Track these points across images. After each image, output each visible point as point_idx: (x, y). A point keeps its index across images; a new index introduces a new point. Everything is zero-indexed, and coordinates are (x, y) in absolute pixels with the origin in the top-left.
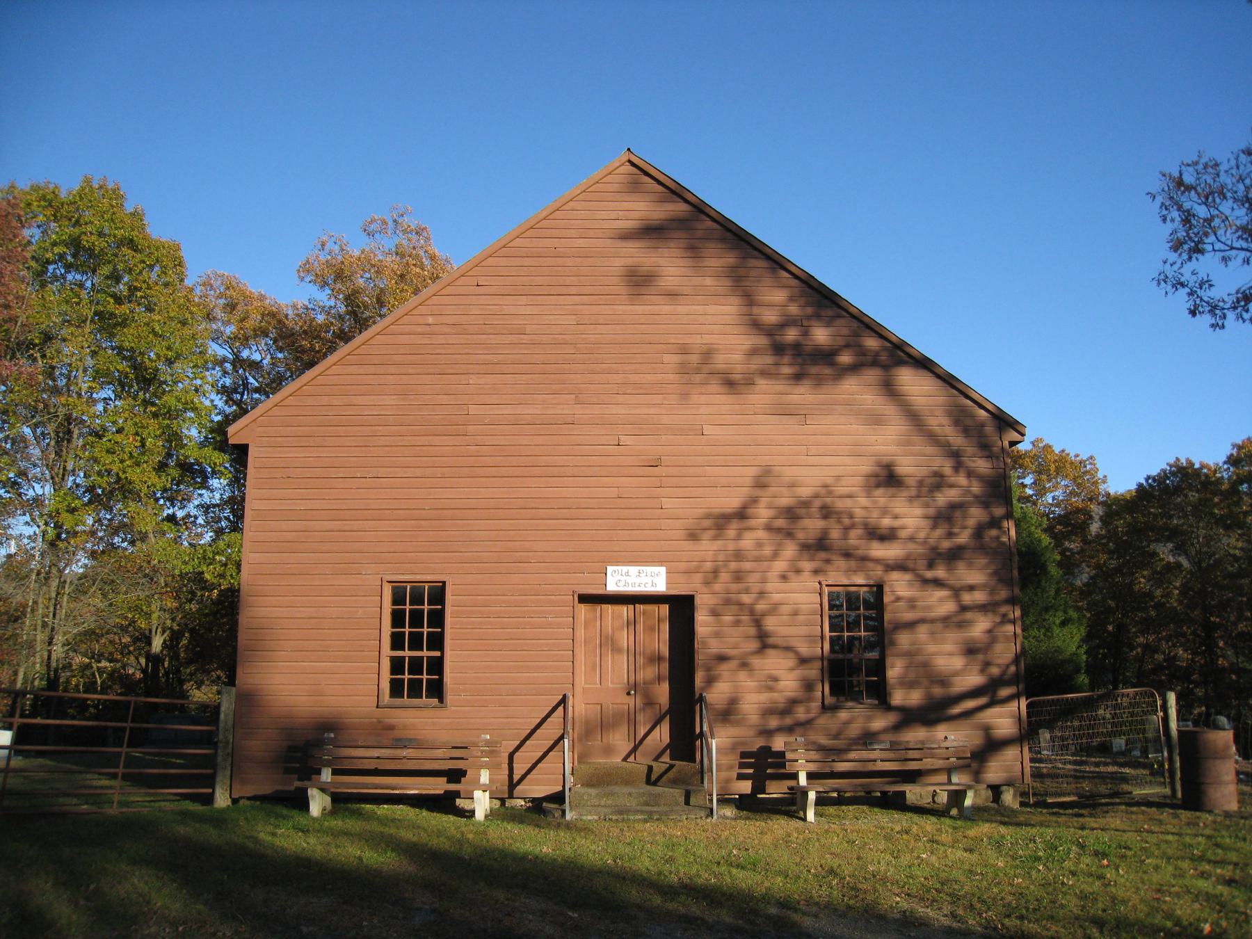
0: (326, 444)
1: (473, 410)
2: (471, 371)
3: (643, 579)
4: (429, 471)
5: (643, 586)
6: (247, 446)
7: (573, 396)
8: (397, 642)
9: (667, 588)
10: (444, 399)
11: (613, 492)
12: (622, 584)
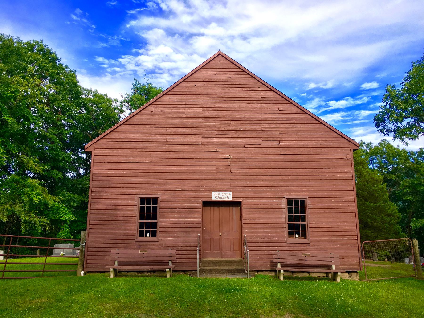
0: (118, 151)
1: (168, 140)
2: (167, 127)
3: (224, 196)
4: (152, 160)
6: (92, 151)
7: (201, 135)
8: (142, 217)
10: (158, 136)
11: (214, 167)
12: (217, 197)
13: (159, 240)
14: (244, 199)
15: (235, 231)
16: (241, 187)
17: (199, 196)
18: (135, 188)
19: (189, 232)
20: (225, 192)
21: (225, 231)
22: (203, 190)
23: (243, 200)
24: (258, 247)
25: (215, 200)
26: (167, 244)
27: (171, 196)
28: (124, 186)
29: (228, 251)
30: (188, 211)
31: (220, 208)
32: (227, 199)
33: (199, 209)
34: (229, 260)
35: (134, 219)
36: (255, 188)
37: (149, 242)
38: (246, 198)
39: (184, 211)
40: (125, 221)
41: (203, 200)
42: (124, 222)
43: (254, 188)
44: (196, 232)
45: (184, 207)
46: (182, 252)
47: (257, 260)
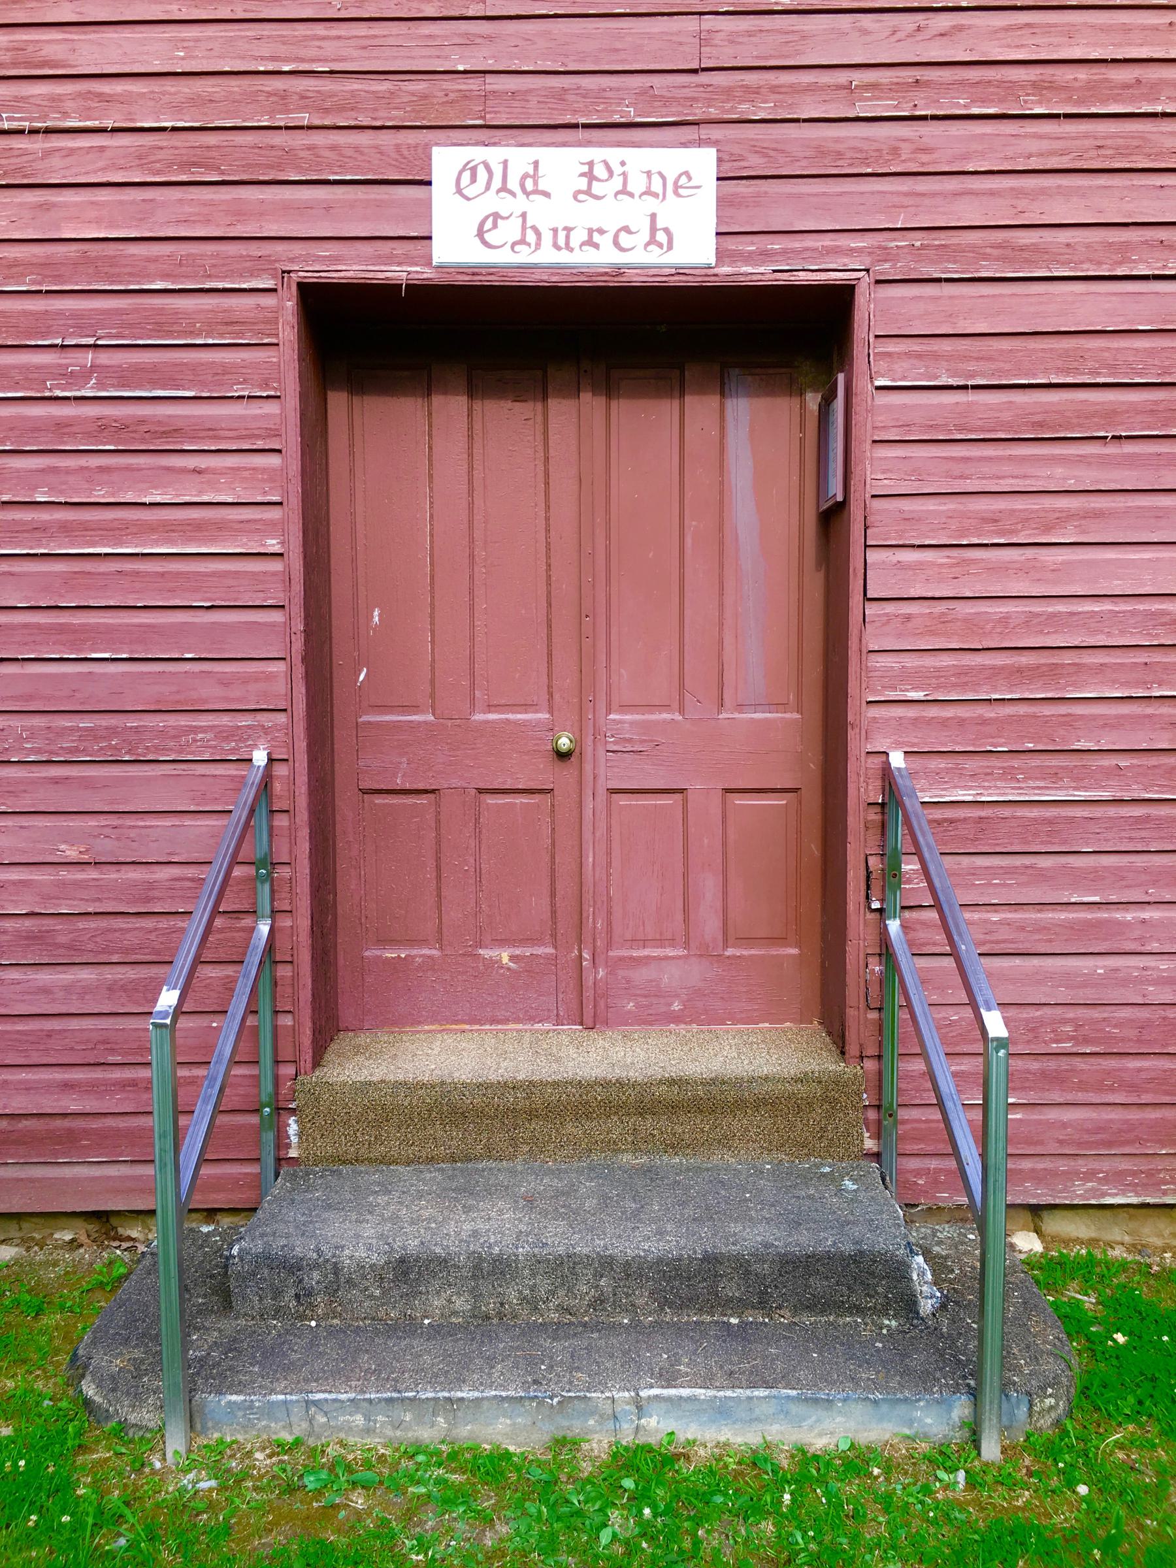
5: (605, 241)
9: (722, 255)
12: (509, 231)
14: (886, 255)
15: (740, 707)
16: (858, 77)
17: (239, 212)
19: (132, 722)
20: (614, 155)
21: (625, 708)
22: (305, 118)
23: (885, 269)
24: (1063, 915)
25: (474, 270)
29: (660, 942)
30: (102, 427)
31: (561, 410)
32: (654, 257)
33: (255, 409)
34: (672, 1082)
36: (1052, 87)
38: (918, 240)
39: (36, 427)
41: (311, 277)
43: (1037, 87)
44: (225, 720)
45: (38, 375)
46: (45, 990)
47: (1044, 1074)
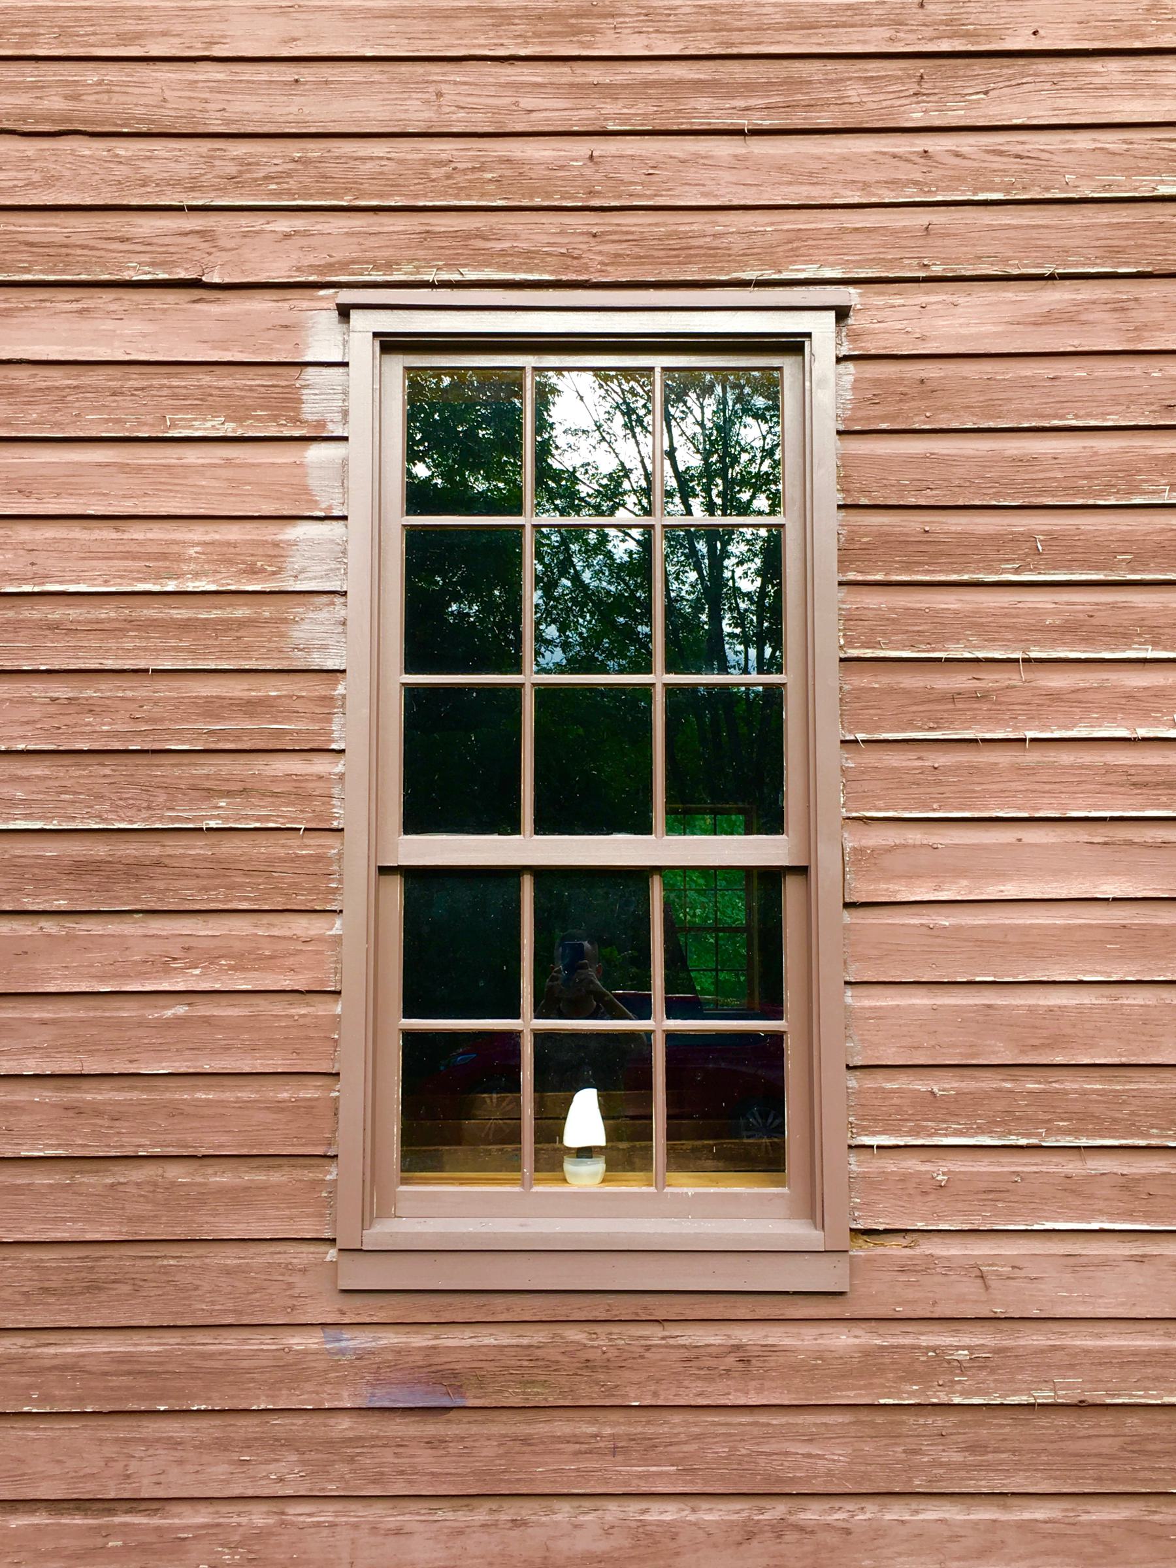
13: (863, 1250)
18: (295, 149)
26: (1035, 1339)
27: (1068, 317)
28: (55, 103)
35: (298, 792)
37: (624, 1307)
40: (100, 849)
42: (81, 869)
